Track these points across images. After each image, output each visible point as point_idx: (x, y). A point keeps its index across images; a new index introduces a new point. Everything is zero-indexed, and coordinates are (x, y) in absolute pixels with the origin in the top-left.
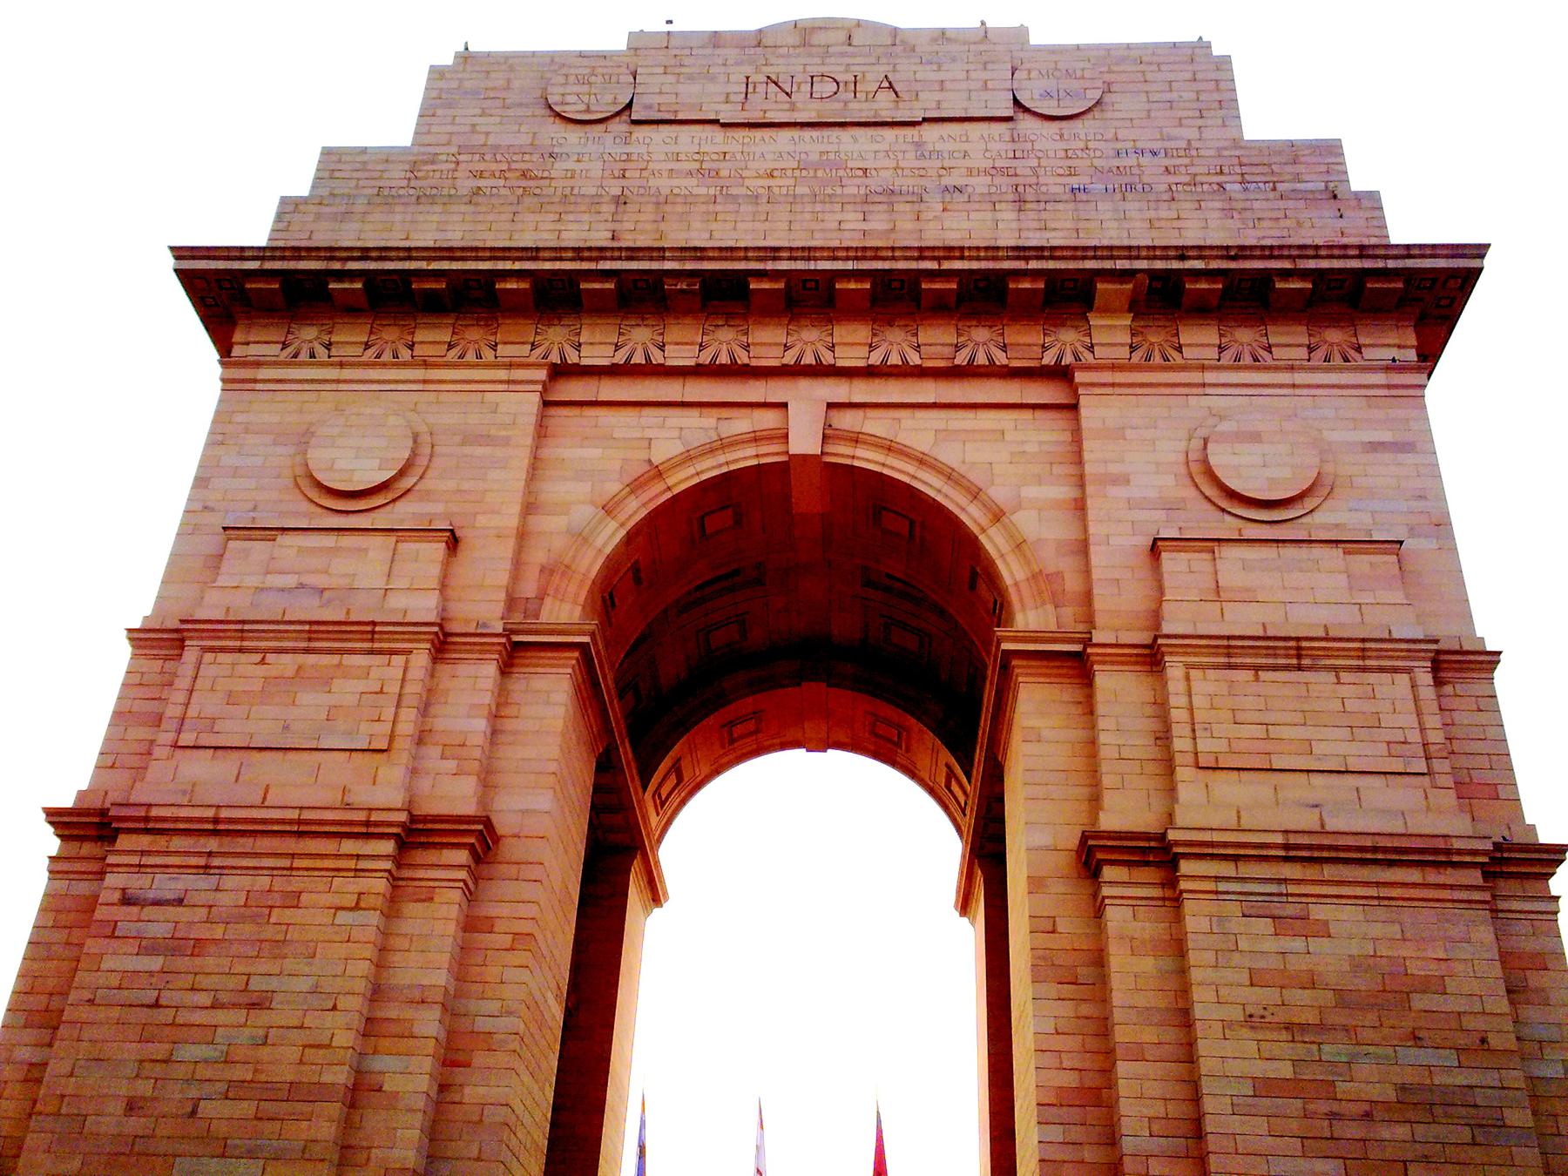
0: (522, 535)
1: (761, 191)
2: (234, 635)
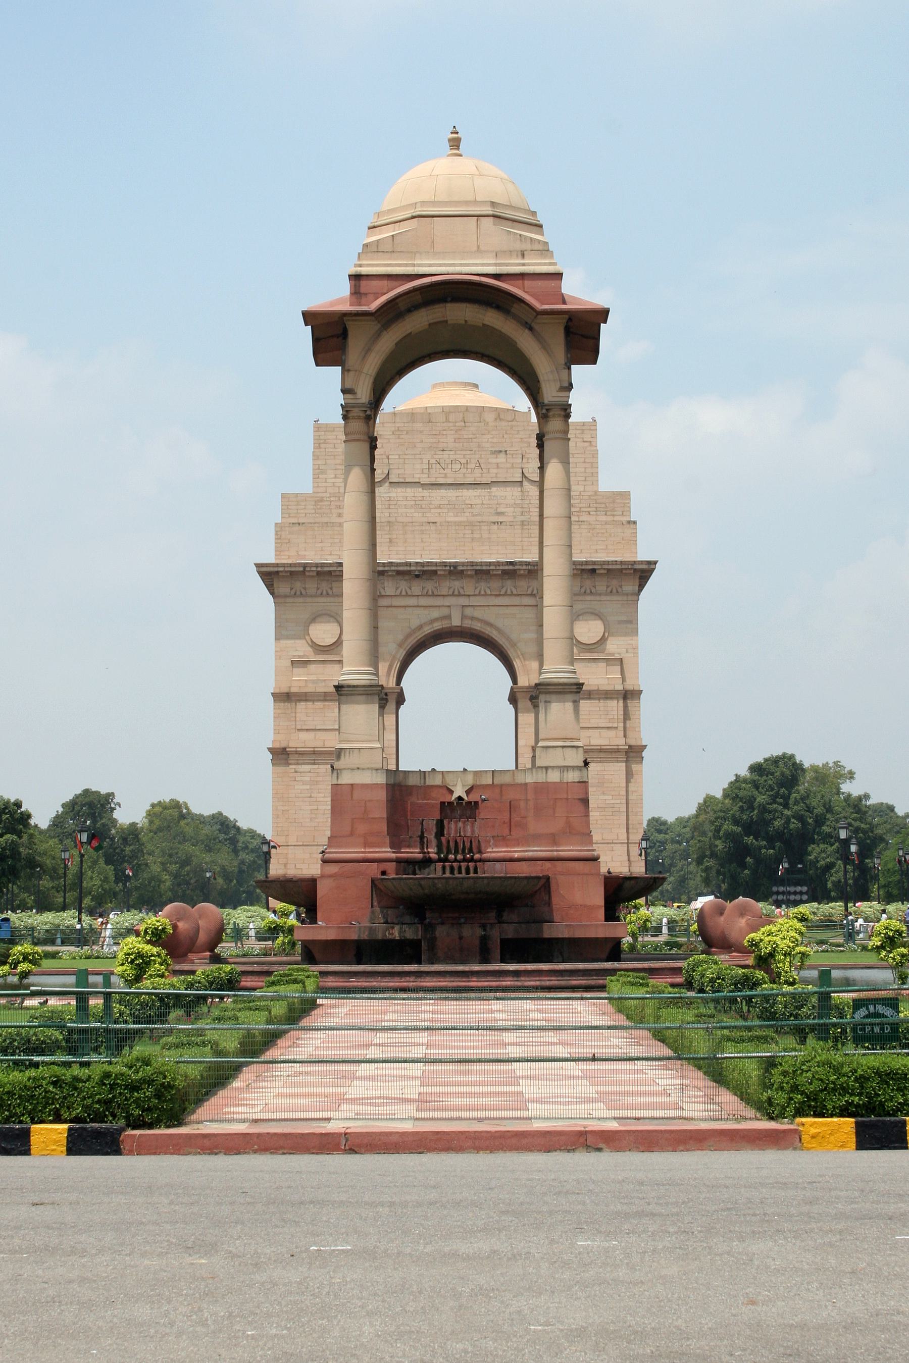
2: (304, 697)
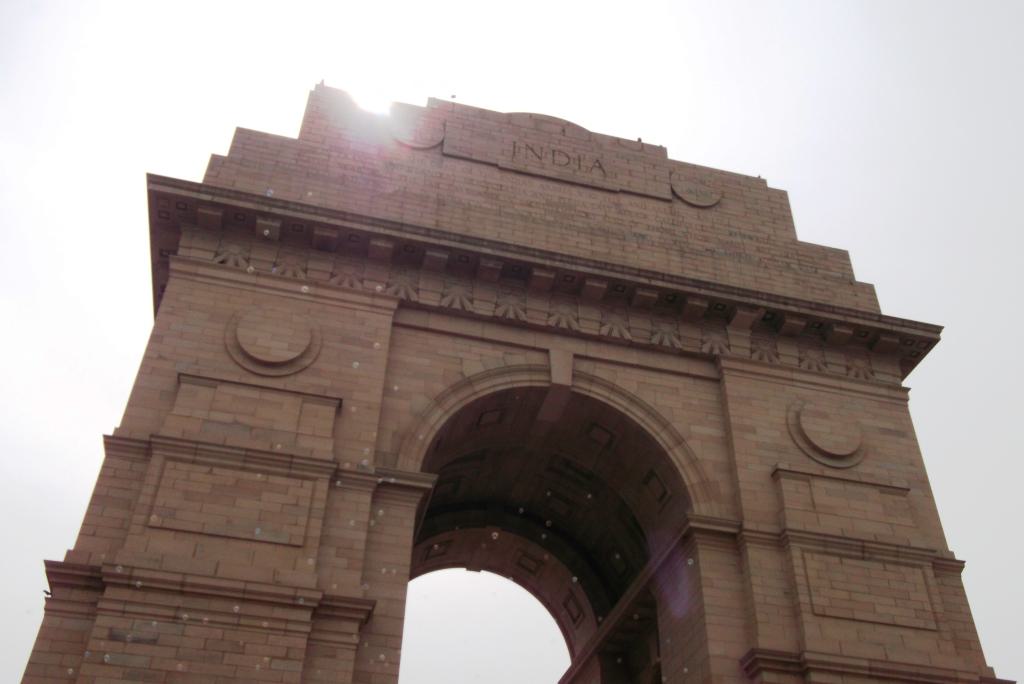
0: (383, 411)
1: (525, 214)
2: (189, 450)
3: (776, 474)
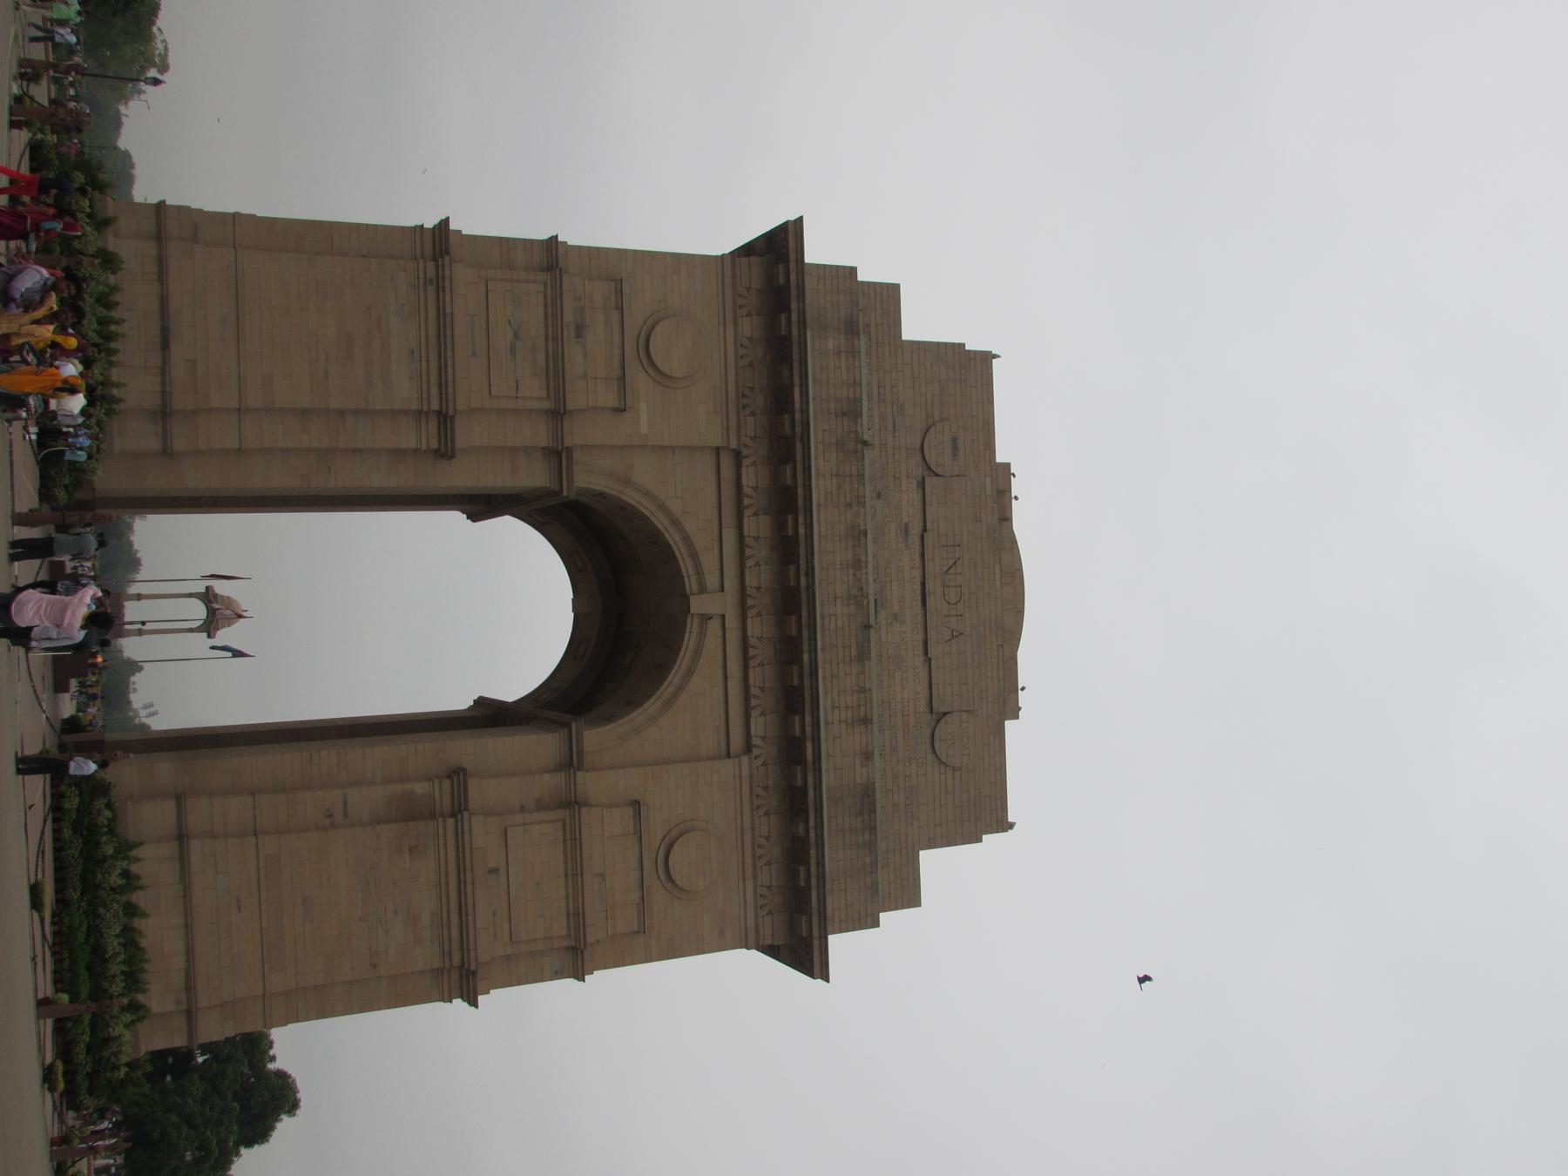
3: (636, 804)
